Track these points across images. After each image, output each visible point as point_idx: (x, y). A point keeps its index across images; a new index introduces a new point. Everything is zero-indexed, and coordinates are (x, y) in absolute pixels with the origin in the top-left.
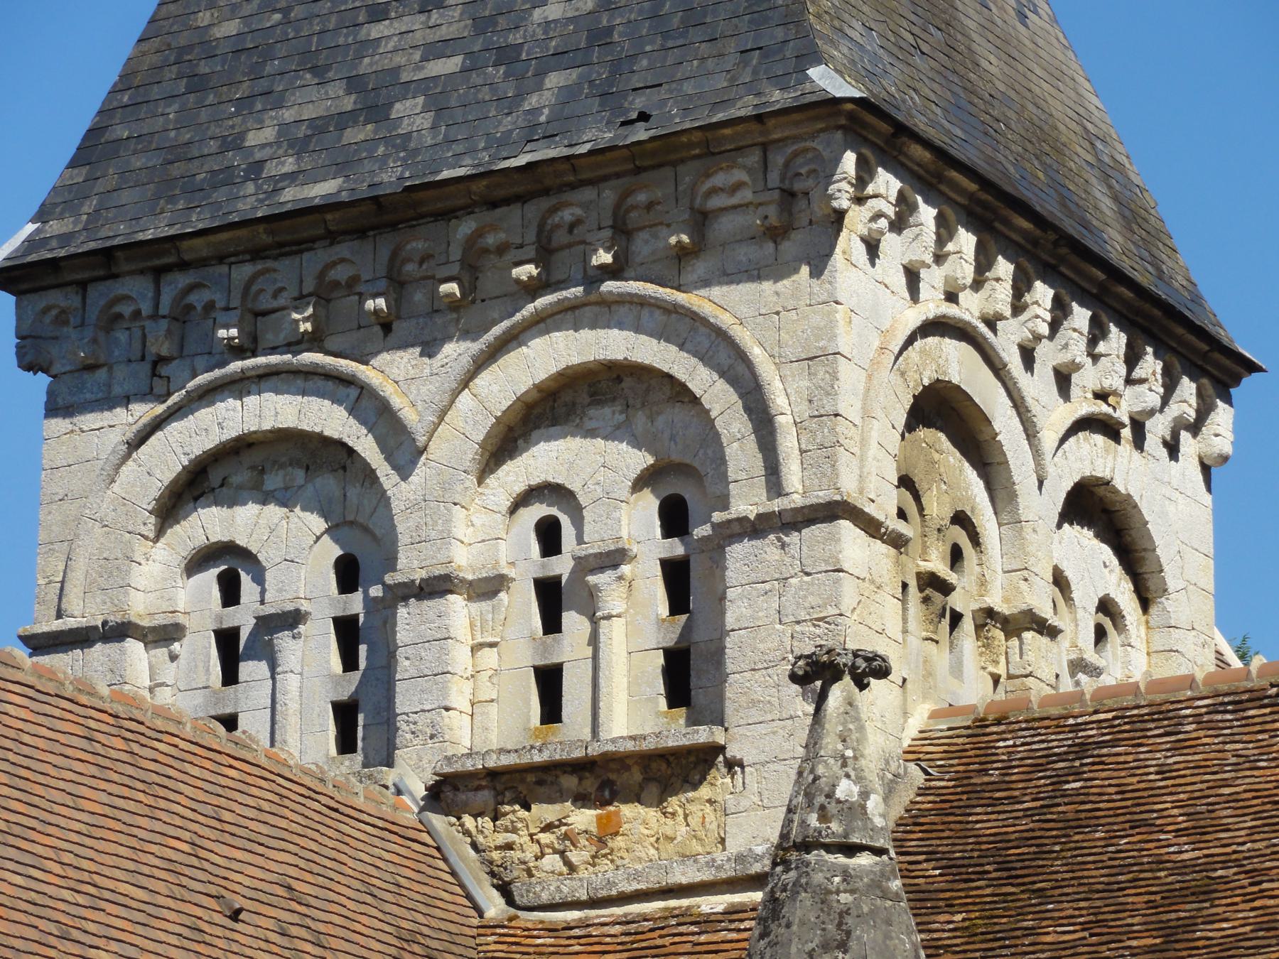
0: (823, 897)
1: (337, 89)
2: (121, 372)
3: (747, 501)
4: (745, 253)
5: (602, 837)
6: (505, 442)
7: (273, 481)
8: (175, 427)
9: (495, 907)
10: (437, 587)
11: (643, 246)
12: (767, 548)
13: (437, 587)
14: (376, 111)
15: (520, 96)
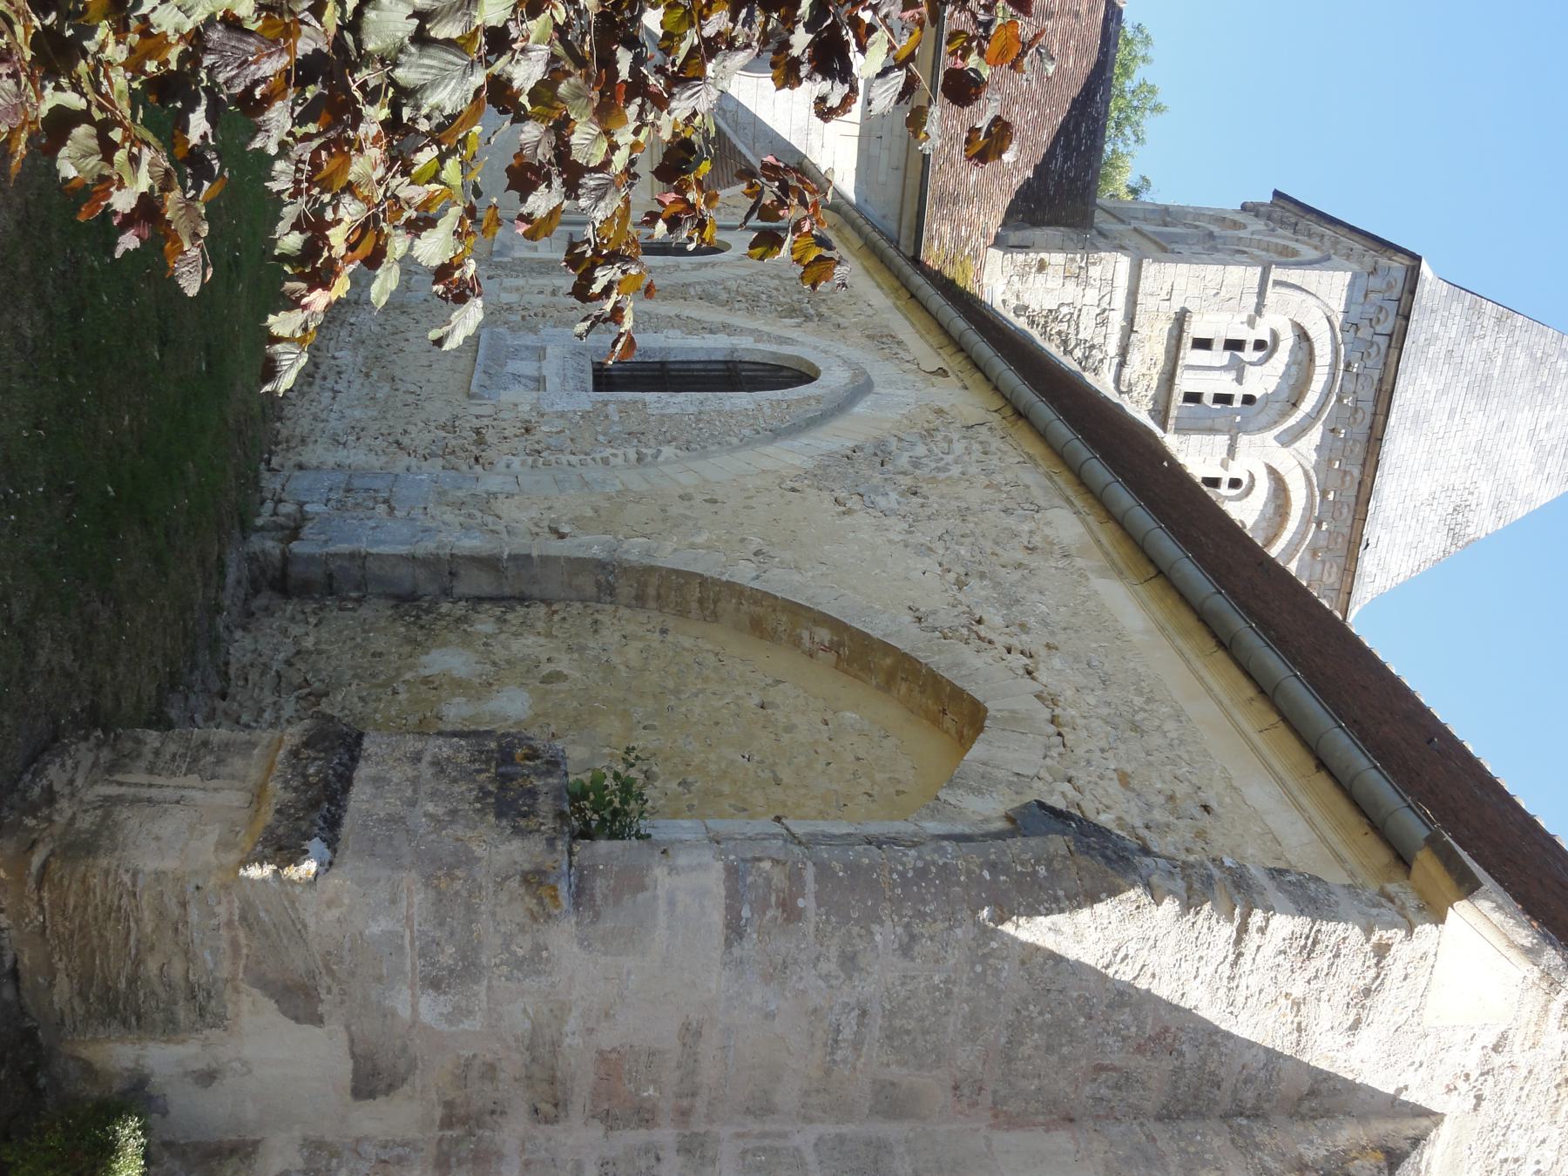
2: (1359, 309)
6: (1272, 471)
8: (1329, 334)
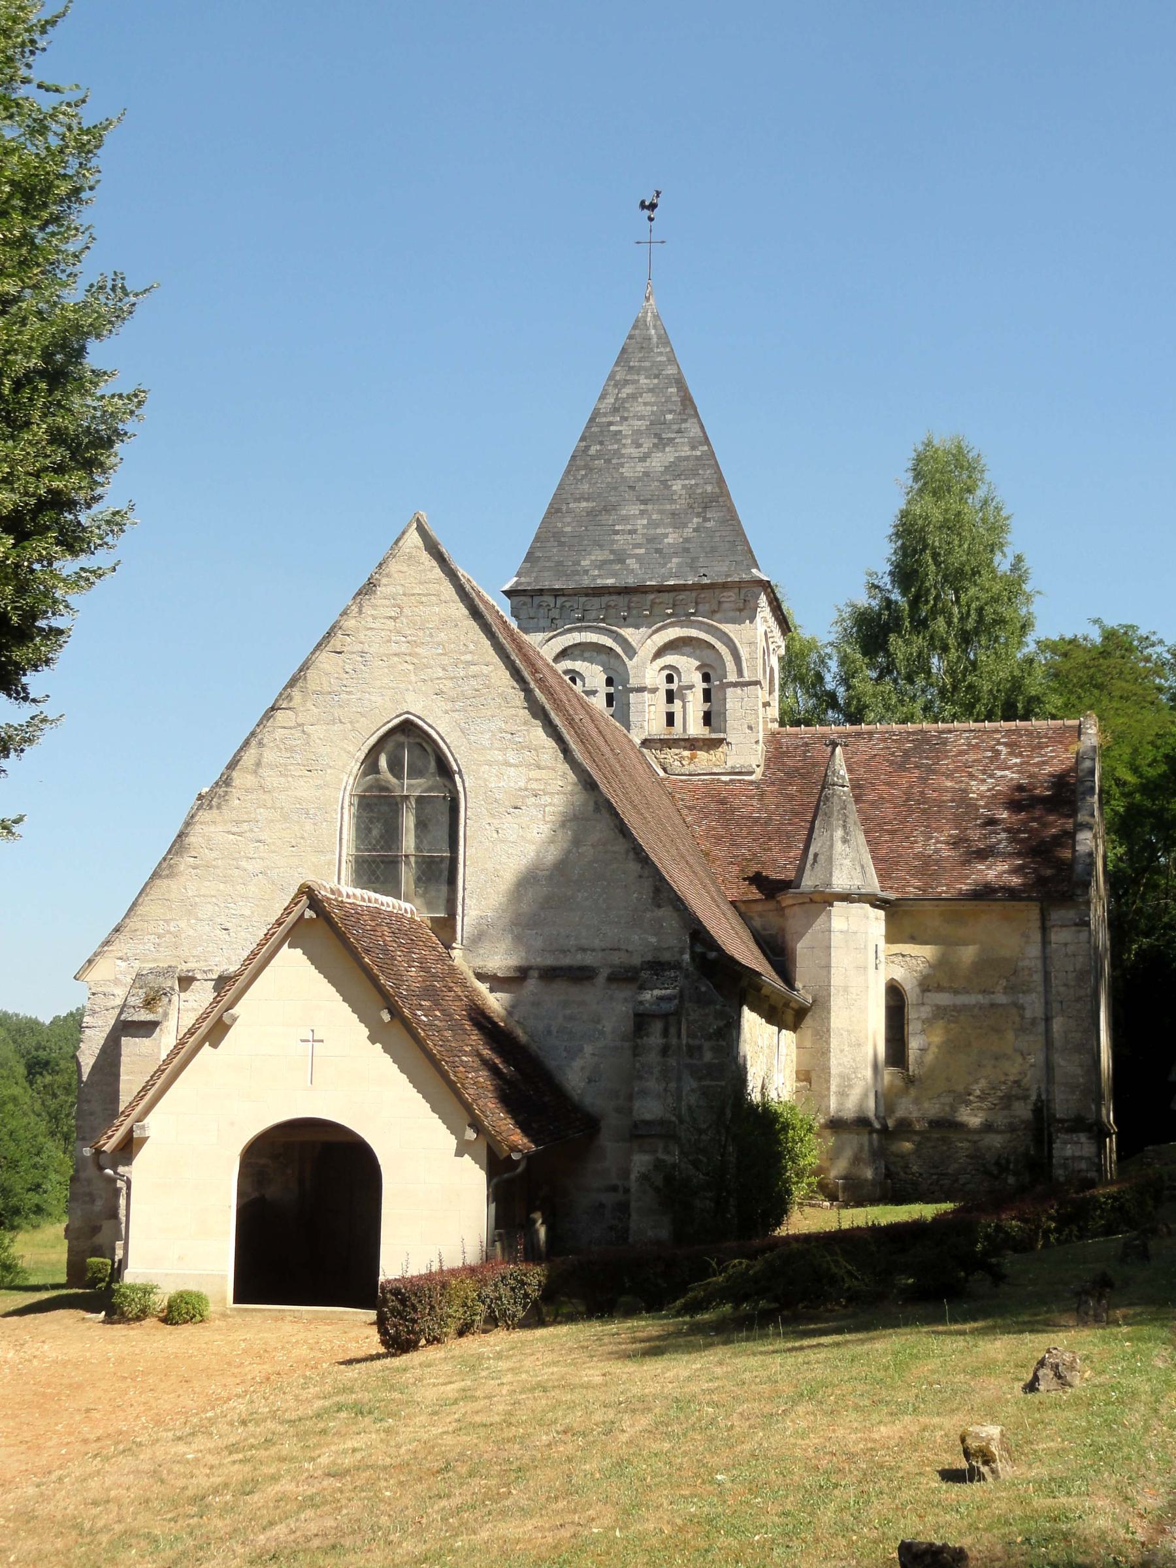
0: (840, 797)
1: (607, 552)
2: (541, 621)
3: (732, 677)
4: (732, 614)
5: (692, 758)
6: (659, 654)
7: (587, 655)
8: (559, 638)
9: (662, 773)
10: (641, 690)
11: (701, 608)
12: (738, 690)
13: (641, 690)
14: (622, 561)
15: (665, 564)
